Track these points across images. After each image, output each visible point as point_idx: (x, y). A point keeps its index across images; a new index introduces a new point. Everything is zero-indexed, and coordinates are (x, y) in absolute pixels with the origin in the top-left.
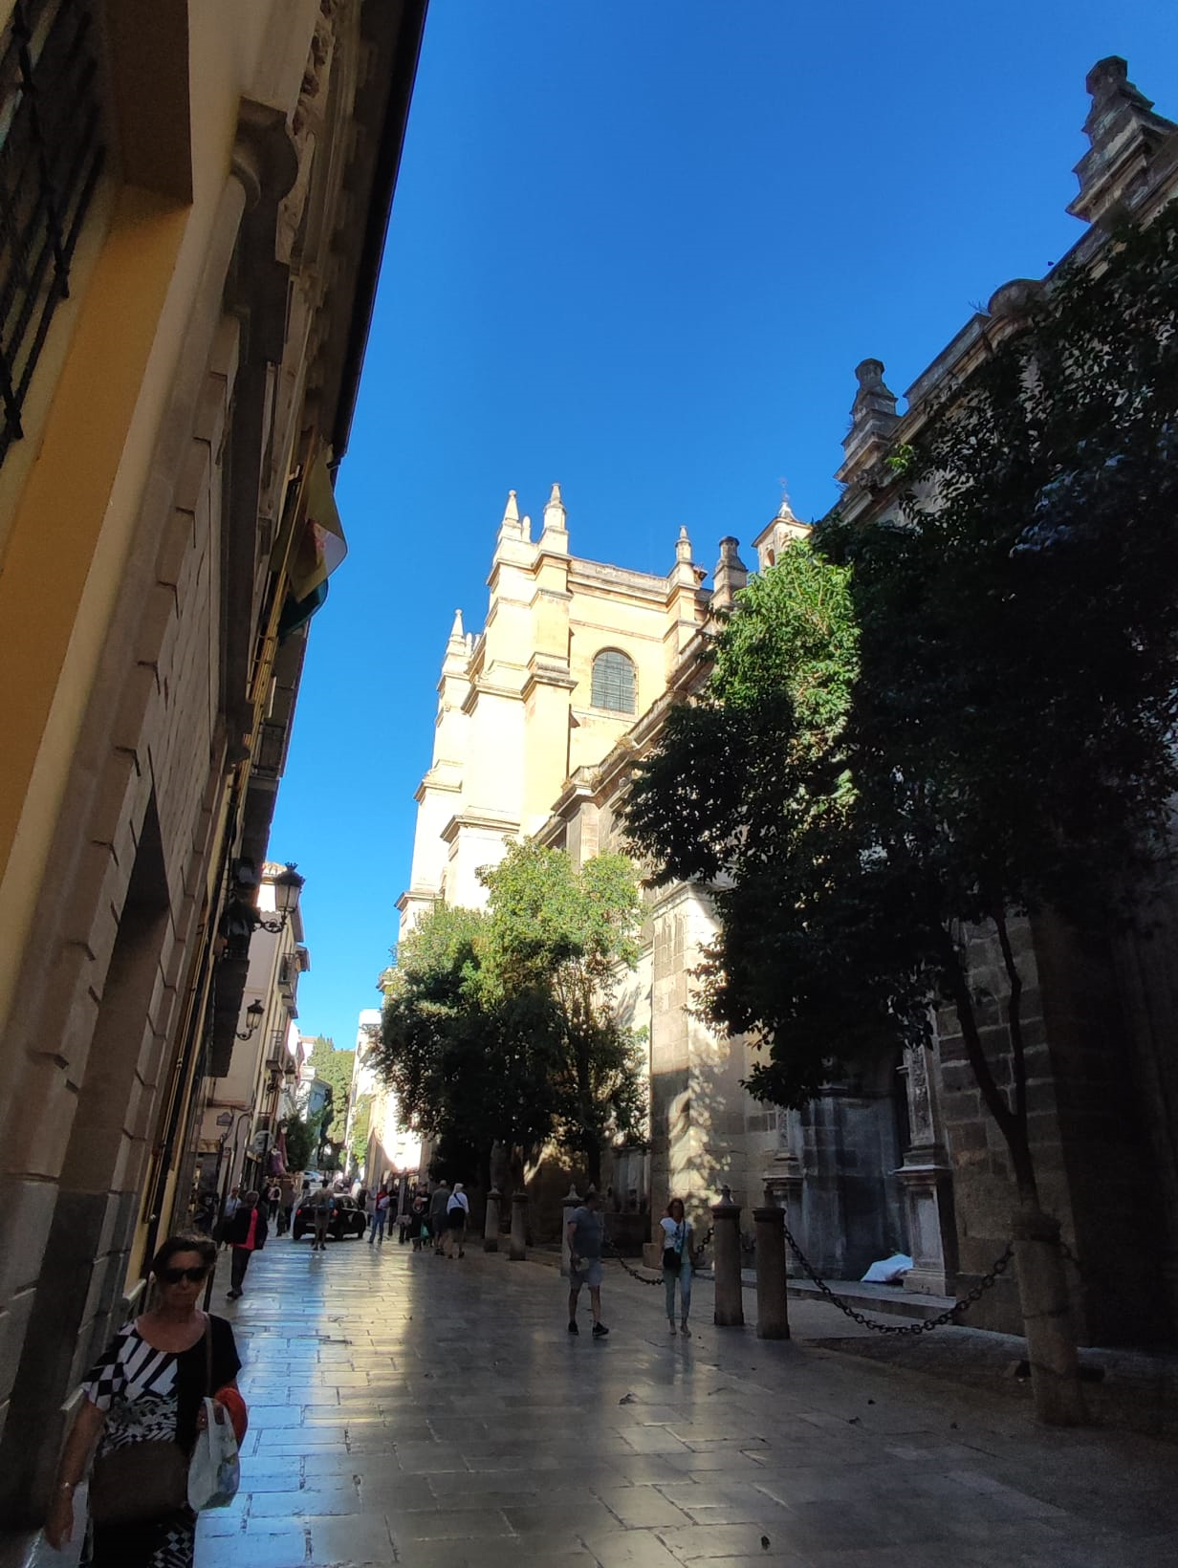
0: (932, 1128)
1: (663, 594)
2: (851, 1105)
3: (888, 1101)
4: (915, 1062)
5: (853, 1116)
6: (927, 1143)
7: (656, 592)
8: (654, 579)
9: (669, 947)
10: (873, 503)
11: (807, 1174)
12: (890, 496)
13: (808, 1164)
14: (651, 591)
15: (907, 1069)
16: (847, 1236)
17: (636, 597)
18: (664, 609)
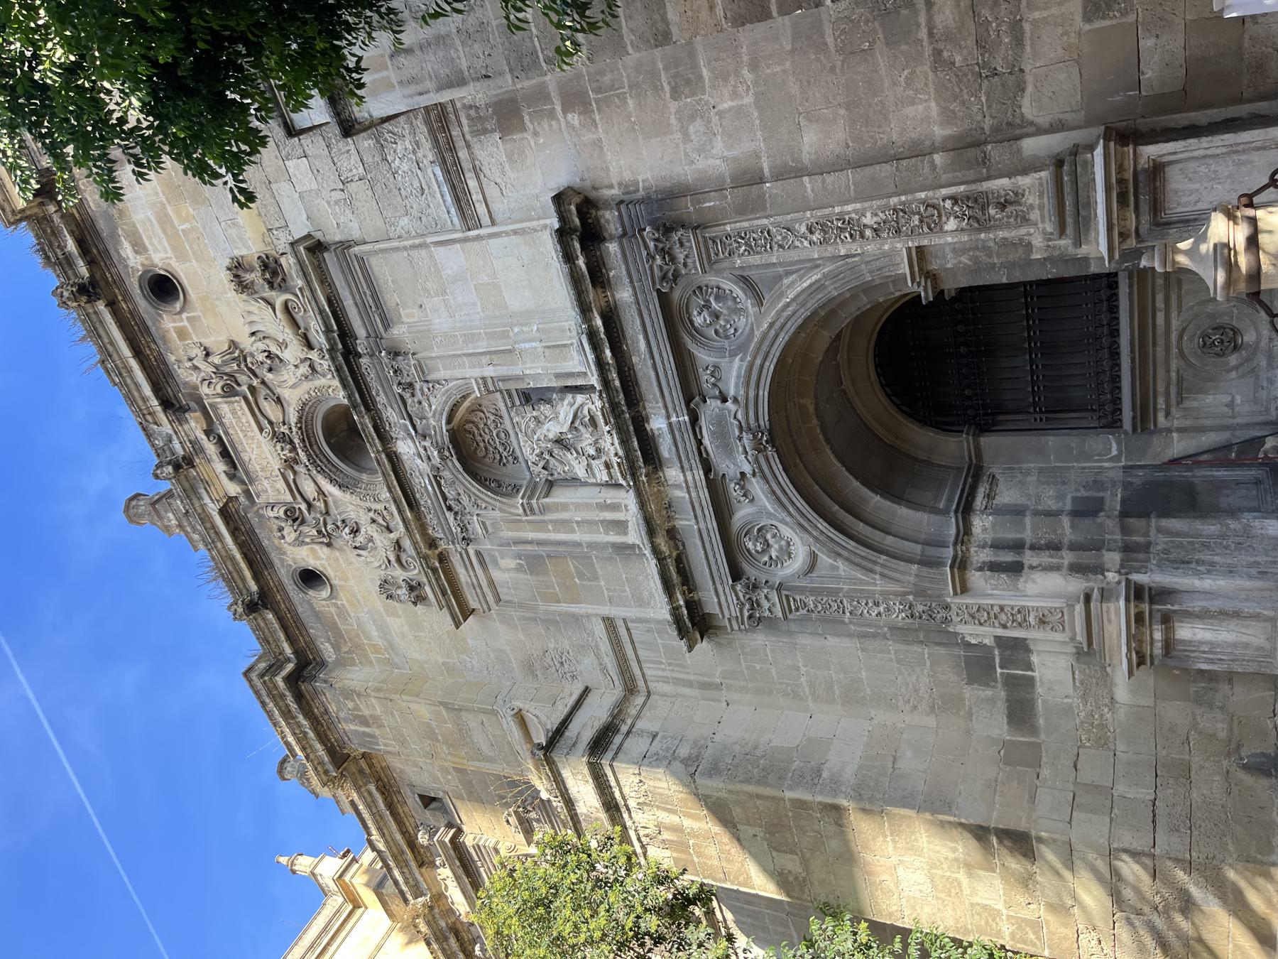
0: (1025, 181)
1: (341, 907)
2: (989, 496)
3: (987, 441)
4: (898, 231)
5: (1007, 495)
6: (1050, 189)
7: (335, 915)
8: (319, 913)
9: (693, 834)
10: (112, 304)
11: (1119, 572)
12: (109, 276)
13: (1099, 569)
14: (330, 921)
15: (909, 249)
16: (1242, 512)
17: (328, 944)
18: (359, 911)
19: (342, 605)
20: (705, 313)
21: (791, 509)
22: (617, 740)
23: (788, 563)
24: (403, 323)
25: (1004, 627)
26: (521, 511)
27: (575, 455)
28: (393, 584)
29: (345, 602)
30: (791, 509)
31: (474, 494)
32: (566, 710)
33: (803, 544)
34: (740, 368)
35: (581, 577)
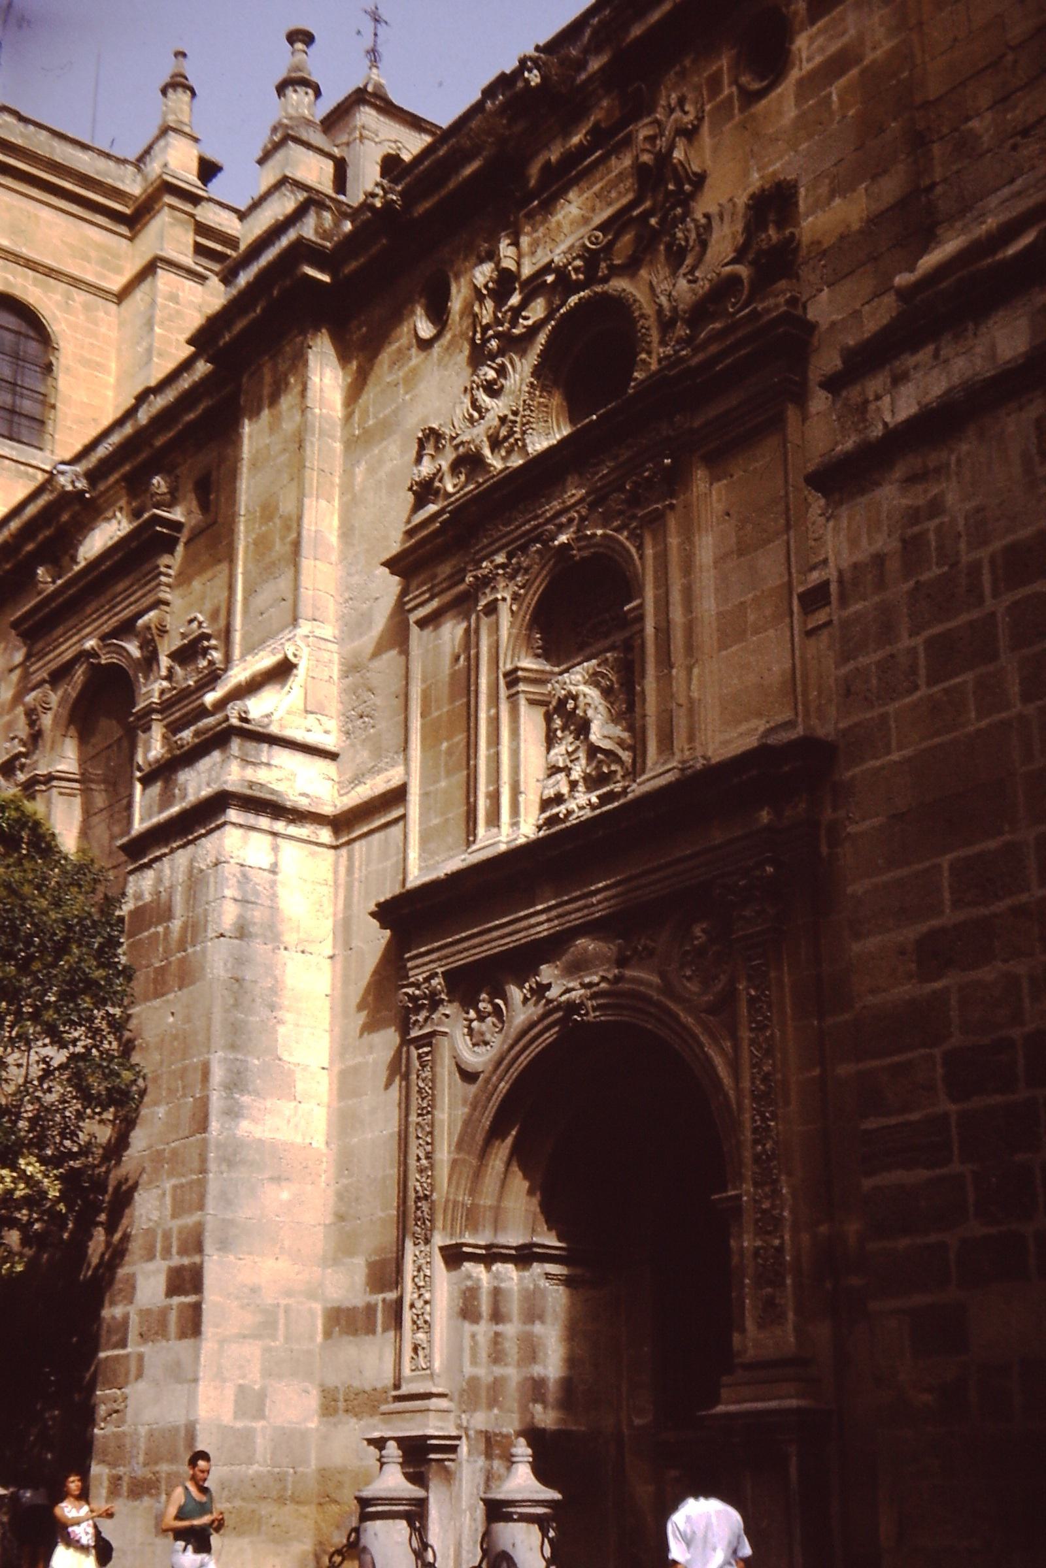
19: (410, 359)
20: (704, 938)
21: (517, 1048)
22: (264, 822)
23: (469, 1043)
24: (711, 484)
25: (412, 1306)
26: (509, 667)
27: (570, 749)
28: (437, 449)
29: (414, 362)
30: (517, 1048)
31: (526, 594)
32: (299, 736)
33: (485, 1063)
34: (649, 985)
35: (450, 753)
